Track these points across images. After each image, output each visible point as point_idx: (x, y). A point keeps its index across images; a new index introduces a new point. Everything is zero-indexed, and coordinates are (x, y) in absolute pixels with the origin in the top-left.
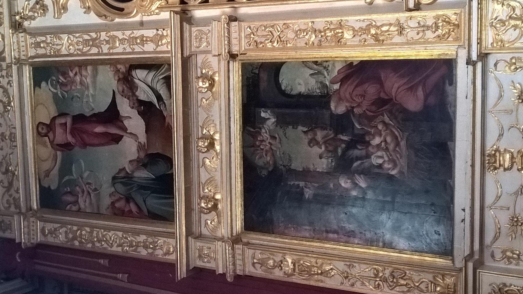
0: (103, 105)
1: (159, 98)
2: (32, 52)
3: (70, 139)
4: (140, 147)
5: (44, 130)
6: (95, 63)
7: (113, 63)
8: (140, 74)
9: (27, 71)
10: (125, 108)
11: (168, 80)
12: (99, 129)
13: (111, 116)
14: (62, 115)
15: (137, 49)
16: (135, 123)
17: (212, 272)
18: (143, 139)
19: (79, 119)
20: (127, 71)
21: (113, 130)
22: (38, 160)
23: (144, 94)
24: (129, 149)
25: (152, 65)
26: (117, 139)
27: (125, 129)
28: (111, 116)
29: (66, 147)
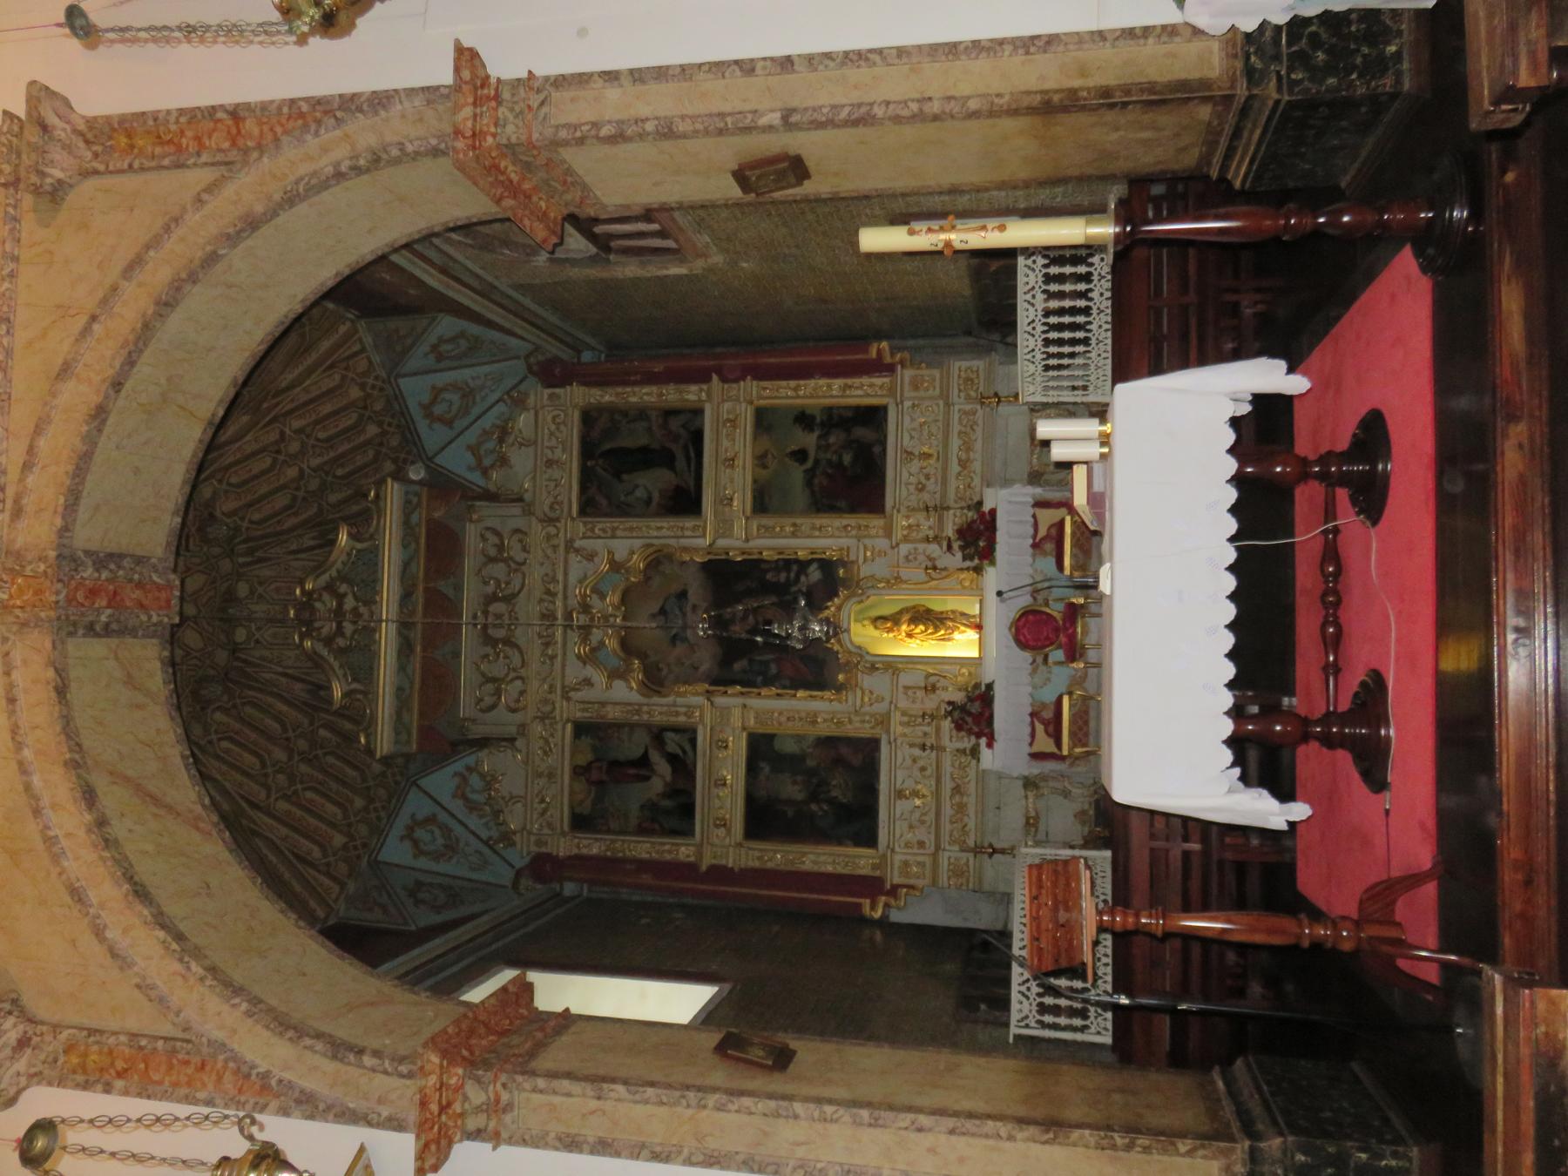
0: (637, 752)
1: (684, 752)
2: (579, 714)
3: (604, 777)
4: (666, 784)
5: (578, 771)
6: (632, 726)
7: (648, 727)
8: (669, 735)
9: (569, 727)
10: (656, 757)
11: (693, 742)
12: (632, 771)
13: (644, 761)
14: (597, 760)
15: (673, 719)
16: (663, 768)
17: (725, 867)
18: (669, 778)
19: (615, 764)
20: (658, 734)
21: (643, 772)
22: (572, 793)
23: (672, 748)
24: (657, 786)
25: (676, 729)
26: (647, 778)
27: (653, 771)
28: (644, 761)
29: (600, 783)
